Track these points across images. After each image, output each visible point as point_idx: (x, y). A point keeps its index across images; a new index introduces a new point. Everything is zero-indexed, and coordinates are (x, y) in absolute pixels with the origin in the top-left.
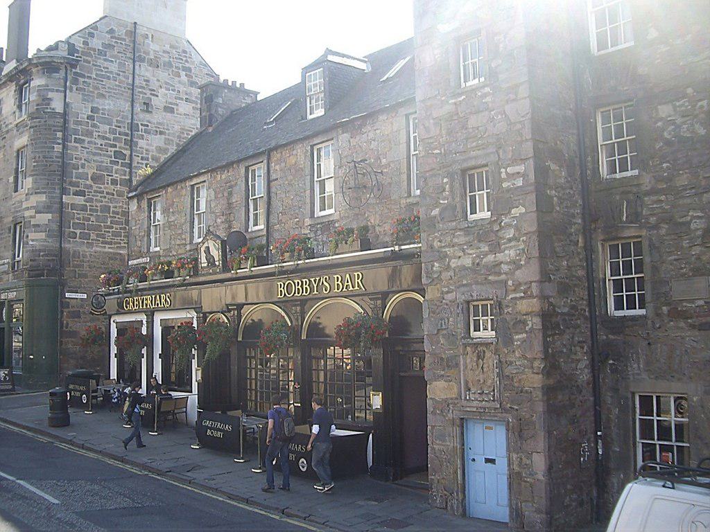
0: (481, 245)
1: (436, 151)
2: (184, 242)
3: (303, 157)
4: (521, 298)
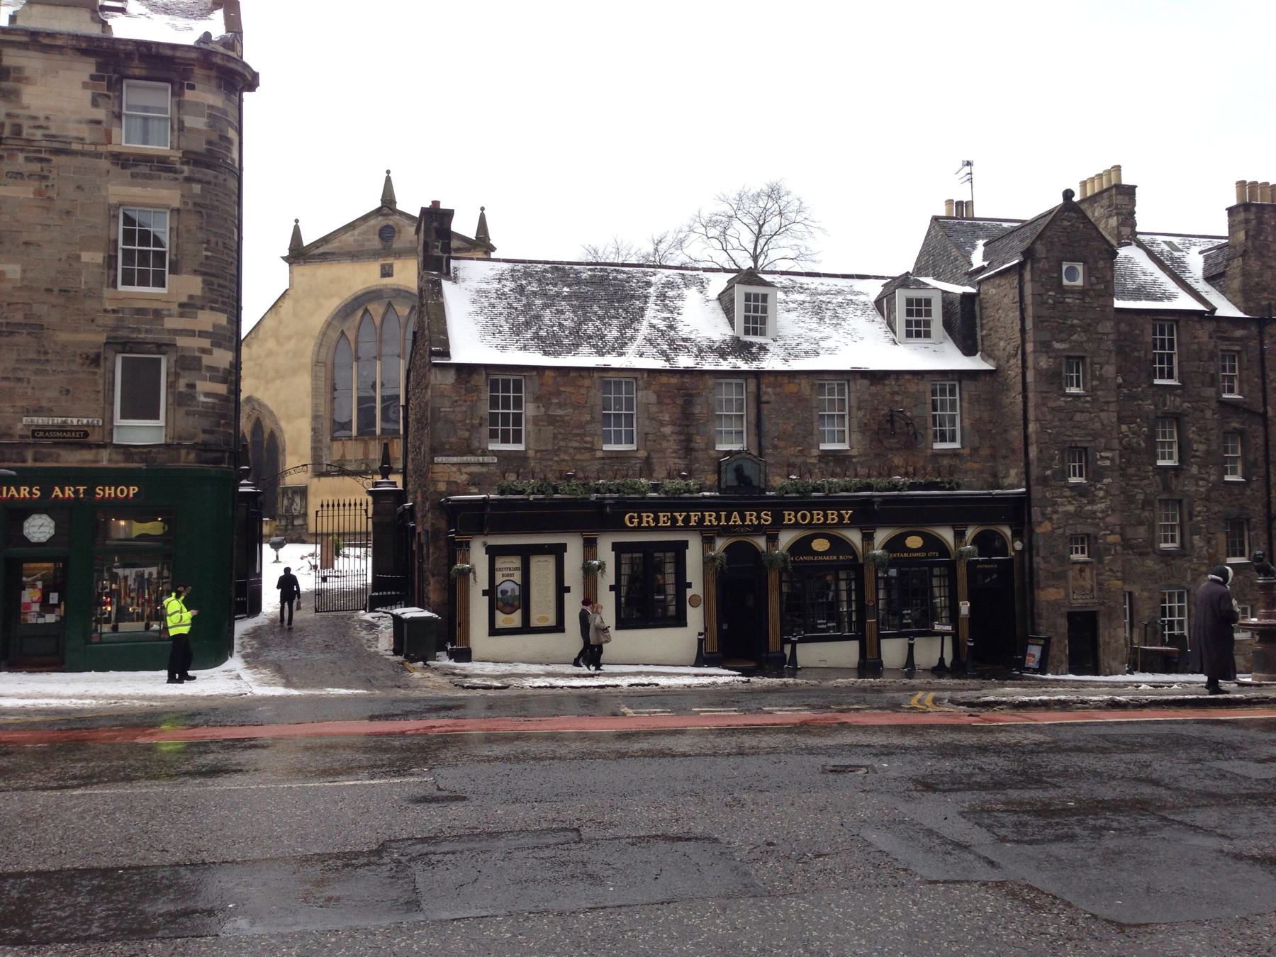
2: (589, 446)
3: (808, 388)
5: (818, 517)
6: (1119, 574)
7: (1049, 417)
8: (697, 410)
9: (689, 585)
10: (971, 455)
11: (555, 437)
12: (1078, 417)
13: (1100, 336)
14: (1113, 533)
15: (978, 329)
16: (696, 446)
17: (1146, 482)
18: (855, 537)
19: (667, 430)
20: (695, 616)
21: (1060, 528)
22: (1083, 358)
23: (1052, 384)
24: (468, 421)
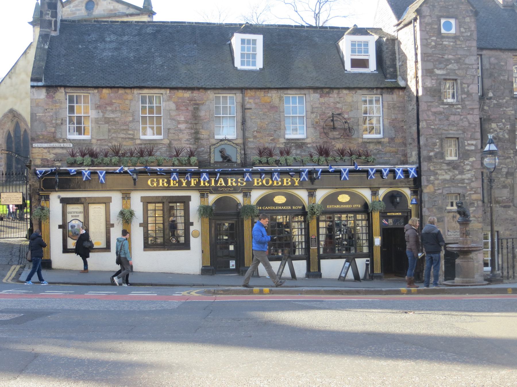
0: (455, 171)
1: (432, 127)
2: (131, 136)
3: (278, 100)
4: (473, 194)
5: (277, 180)
6: (479, 219)
7: (432, 118)
8: (202, 114)
9: (192, 224)
10: (389, 143)
11: (109, 131)
12: (452, 118)
13: (467, 66)
14: (476, 193)
15: (397, 61)
16: (202, 136)
17: (509, 160)
18: (303, 195)
19: (182, 126)
20: (195, 243)
21: (439, 189)
22: (456, 80)
23: (435, 96)
24: (54, 122)
